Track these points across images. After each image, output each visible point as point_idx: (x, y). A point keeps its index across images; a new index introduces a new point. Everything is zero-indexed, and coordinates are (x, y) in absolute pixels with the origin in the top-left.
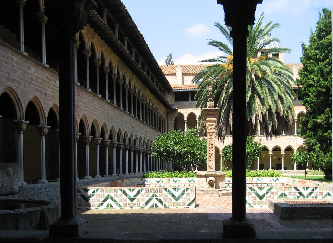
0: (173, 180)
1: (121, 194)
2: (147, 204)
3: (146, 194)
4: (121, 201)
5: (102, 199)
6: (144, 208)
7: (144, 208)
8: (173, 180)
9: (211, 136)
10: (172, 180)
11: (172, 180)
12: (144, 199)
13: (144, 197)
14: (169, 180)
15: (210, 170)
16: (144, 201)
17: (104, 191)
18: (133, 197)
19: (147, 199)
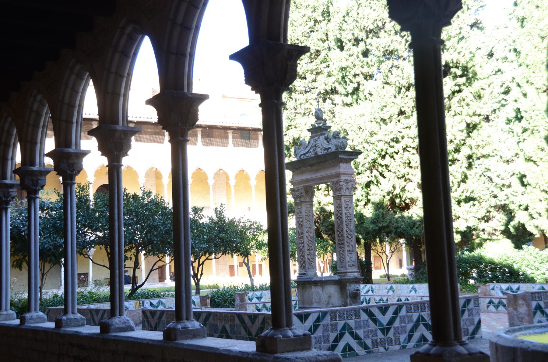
0: (151, 304)
1: (368, 321)
2: (410, 337)
3: (408, 316)
4: (366, 336)
5: (333, 336)
6: (407, 347)
7: (406, 346)
8: (151, 304)
9: (348, 203)
10: (147, 303)
11: (147, 303)
12: (405, 327)
13: (405, 322)
14: (141, 305)
15: (350, 271)
16: (406, 332)
17: (336, 317)
18: (387, 325)
19: (409, 326)
